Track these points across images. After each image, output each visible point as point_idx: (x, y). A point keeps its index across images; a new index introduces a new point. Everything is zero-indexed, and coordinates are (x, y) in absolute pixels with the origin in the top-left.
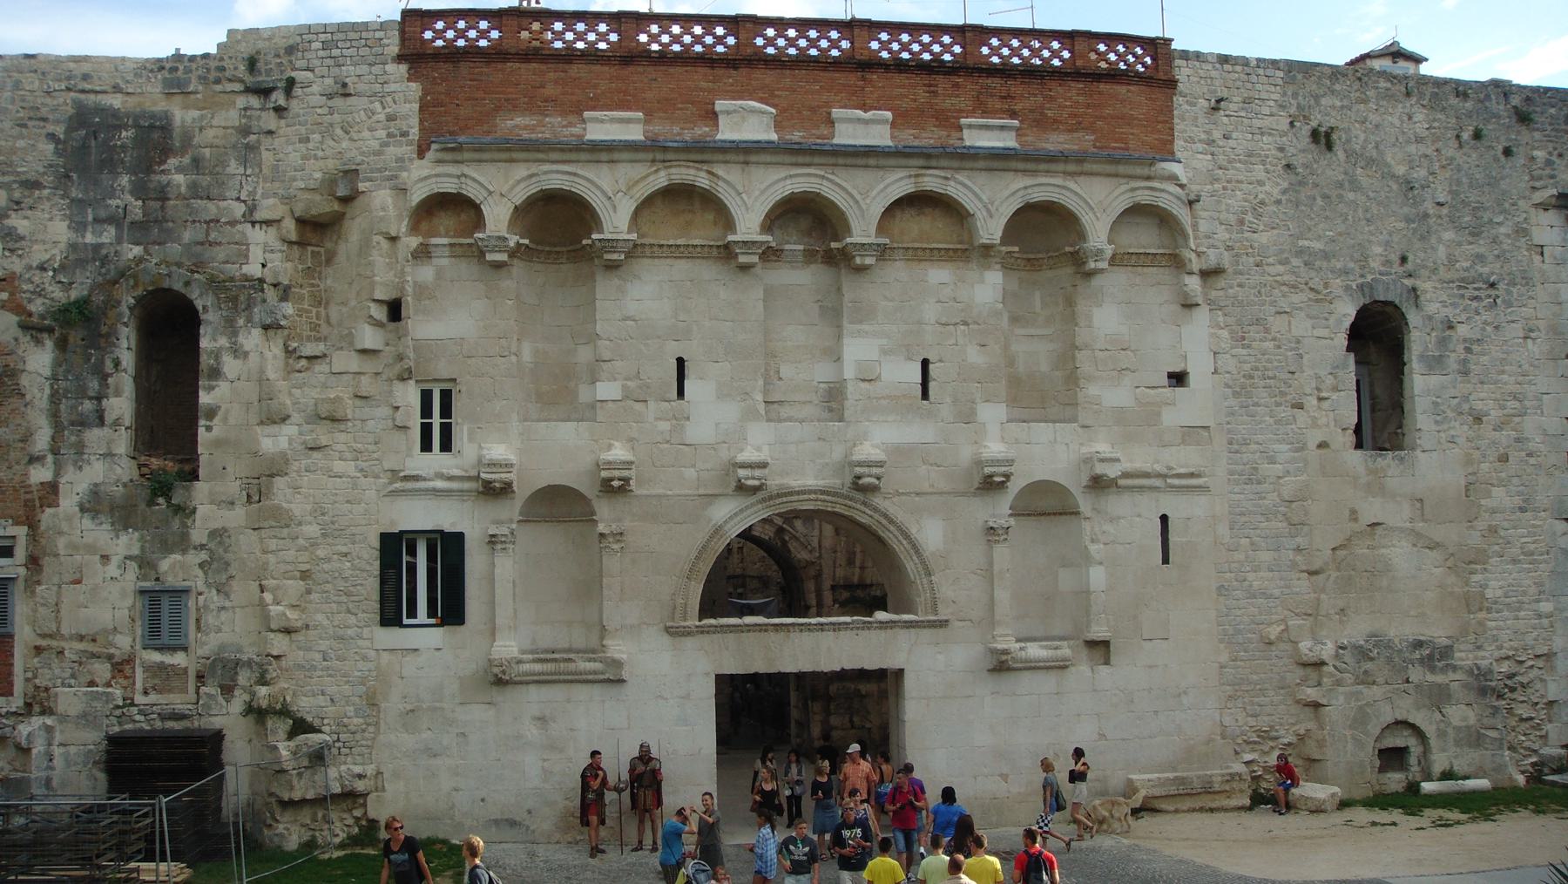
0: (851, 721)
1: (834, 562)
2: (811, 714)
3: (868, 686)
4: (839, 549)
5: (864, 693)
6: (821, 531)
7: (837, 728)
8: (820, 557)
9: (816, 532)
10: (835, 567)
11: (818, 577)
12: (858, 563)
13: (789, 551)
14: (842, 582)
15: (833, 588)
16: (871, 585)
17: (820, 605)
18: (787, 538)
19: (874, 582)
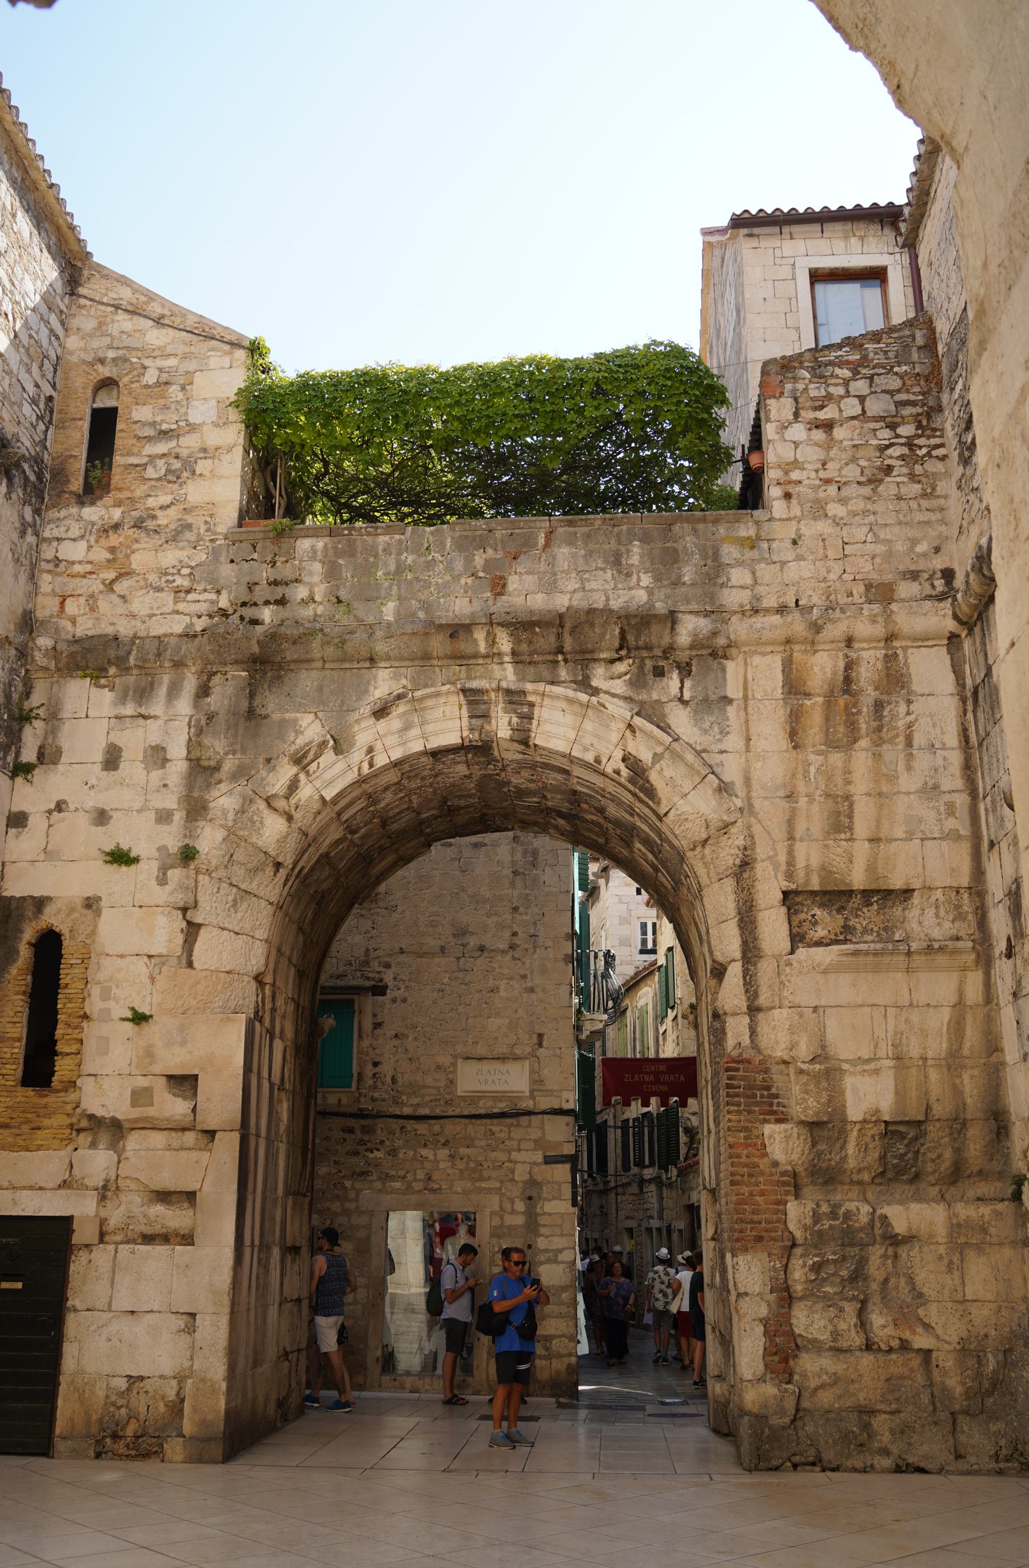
0: (863, 1323)
1: (791, 823)
2: (733, 1298)
3: (914, 1206)
4: (801, 787)
5: (900, 1227)
6: (748, 740)
7: (816, 1346)
8: (748, 809)
9: (734, 741)
10: (791, 838)
11: (746, 864)
12: (862, 827)
13: (650, 792)
14: (815, 885)
15: (786, 894)
16: (907, 893)
17: (750, 952)
18: (645, 755)
19: (916, 884)
